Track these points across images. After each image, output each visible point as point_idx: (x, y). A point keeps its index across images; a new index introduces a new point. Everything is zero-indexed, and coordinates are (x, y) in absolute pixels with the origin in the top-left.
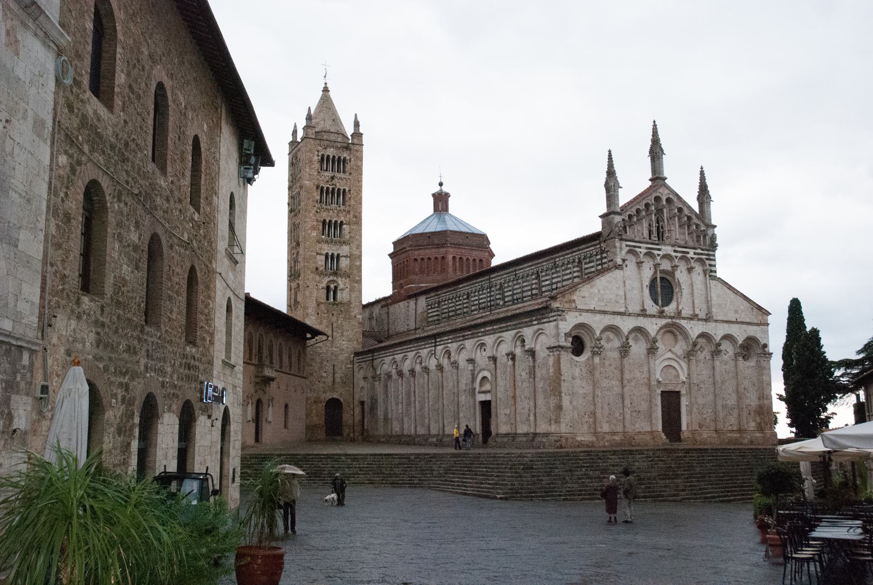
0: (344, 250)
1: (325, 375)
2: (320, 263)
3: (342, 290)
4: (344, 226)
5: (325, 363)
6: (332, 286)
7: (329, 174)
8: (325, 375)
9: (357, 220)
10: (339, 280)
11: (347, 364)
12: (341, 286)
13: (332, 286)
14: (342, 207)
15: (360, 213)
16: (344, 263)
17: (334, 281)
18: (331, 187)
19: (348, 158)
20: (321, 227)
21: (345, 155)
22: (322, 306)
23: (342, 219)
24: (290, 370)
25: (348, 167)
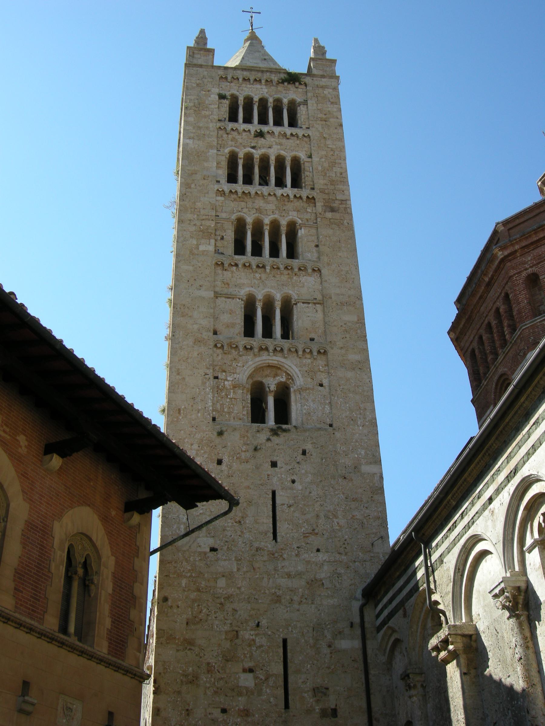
0: (303, 287)
1: (247, 681)
2: (225, 318)
3: (300, 390)
4: (301, 233)
5: (247, 634)
6: (272, 384)
7: (255, 126)
8: (247, 681)
9: (338, 209)
10: (292, 365)
11: (338, 634)
12: (300, 381)
13: (272, 384)
14: (288, 190)
15: (346, 202)
16: (304, 319)
17: (276, 368)
18: (257, 154)
19: (299, 100)
20: (230, 236)
21: (289, 94)
22: (234, 439)
23: (293, 216)
24: (64, 629)
25: (302, 112)
